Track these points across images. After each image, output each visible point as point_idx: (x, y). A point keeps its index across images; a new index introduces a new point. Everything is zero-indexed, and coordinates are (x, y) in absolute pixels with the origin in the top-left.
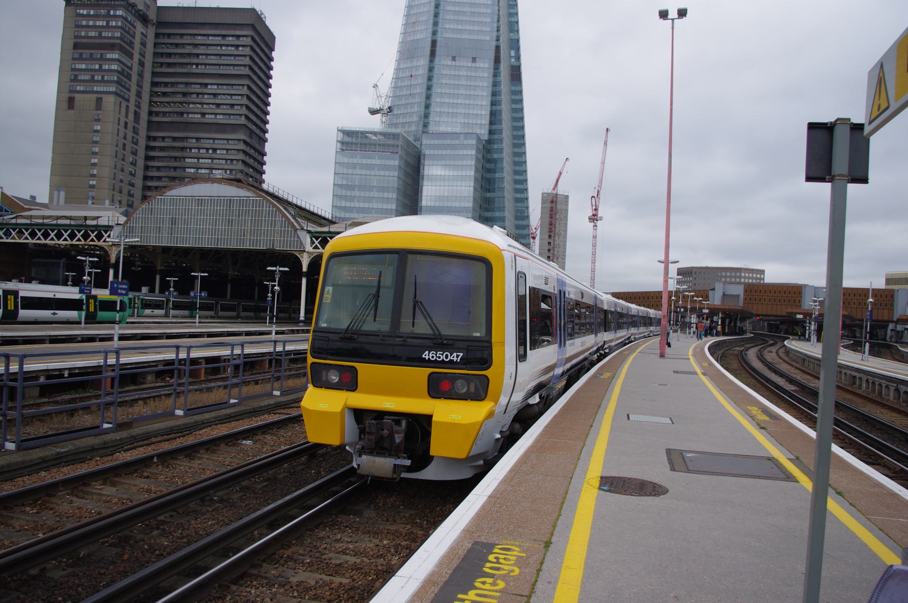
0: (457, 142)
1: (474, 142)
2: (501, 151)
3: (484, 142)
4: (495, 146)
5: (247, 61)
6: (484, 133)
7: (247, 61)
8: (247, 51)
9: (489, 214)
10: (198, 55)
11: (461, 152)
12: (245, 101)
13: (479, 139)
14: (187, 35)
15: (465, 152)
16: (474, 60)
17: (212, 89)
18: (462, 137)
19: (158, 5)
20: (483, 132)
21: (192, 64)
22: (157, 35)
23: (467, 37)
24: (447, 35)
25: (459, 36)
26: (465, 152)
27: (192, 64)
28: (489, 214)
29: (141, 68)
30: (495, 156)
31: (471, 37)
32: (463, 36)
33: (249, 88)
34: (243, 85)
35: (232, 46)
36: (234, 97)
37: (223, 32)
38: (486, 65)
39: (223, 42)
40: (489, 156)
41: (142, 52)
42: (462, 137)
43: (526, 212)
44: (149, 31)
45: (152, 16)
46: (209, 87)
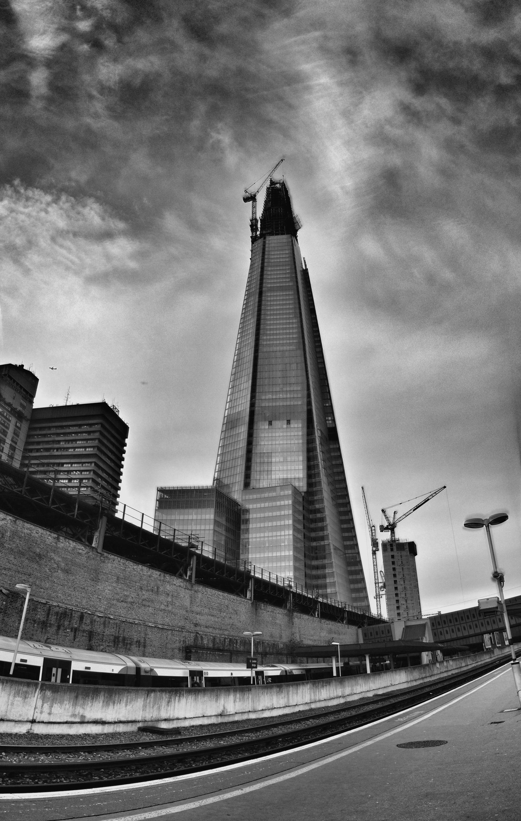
0: (274, 494)
1: (290, 492)
2: (322, 501)
3: (303, 494)
4: (316, 498)
5: (96, 443)
6: (302, 486)
7: (96, 443)
8: (97, 435)
9: (315, 563)
10: (59, 442)
11: (278, 503)
12: (91, 475)
13: (296, 491)
14: (53, 427)
15: (282, 503)
16: (289, 422)
17: (66, 467)
18: (278, 489)
19: (34, 407)
20: (301, 484)
21: (54, 449)
22: (30, 429)
23: (281, 404)
24: (263, 405)
25: (274, 404)
26: (282, 503)
27: (54, 449)
28: (315, 563)
29: (12, 452)
30: (317, 506)
31: (285, 404)
32: (278, 404)
33: (96, 464)
34: (91, 463)
35: (85, 432)
36: (83, 473)
37: (80, 422)
38: (300, 425)
39: (79, 430)
40: (311, 507)
41: (14, 440)
42: (278, 489)
43: (358, 557)
44: (23, 425)
45: (27, 414)
46: (65, 465)
